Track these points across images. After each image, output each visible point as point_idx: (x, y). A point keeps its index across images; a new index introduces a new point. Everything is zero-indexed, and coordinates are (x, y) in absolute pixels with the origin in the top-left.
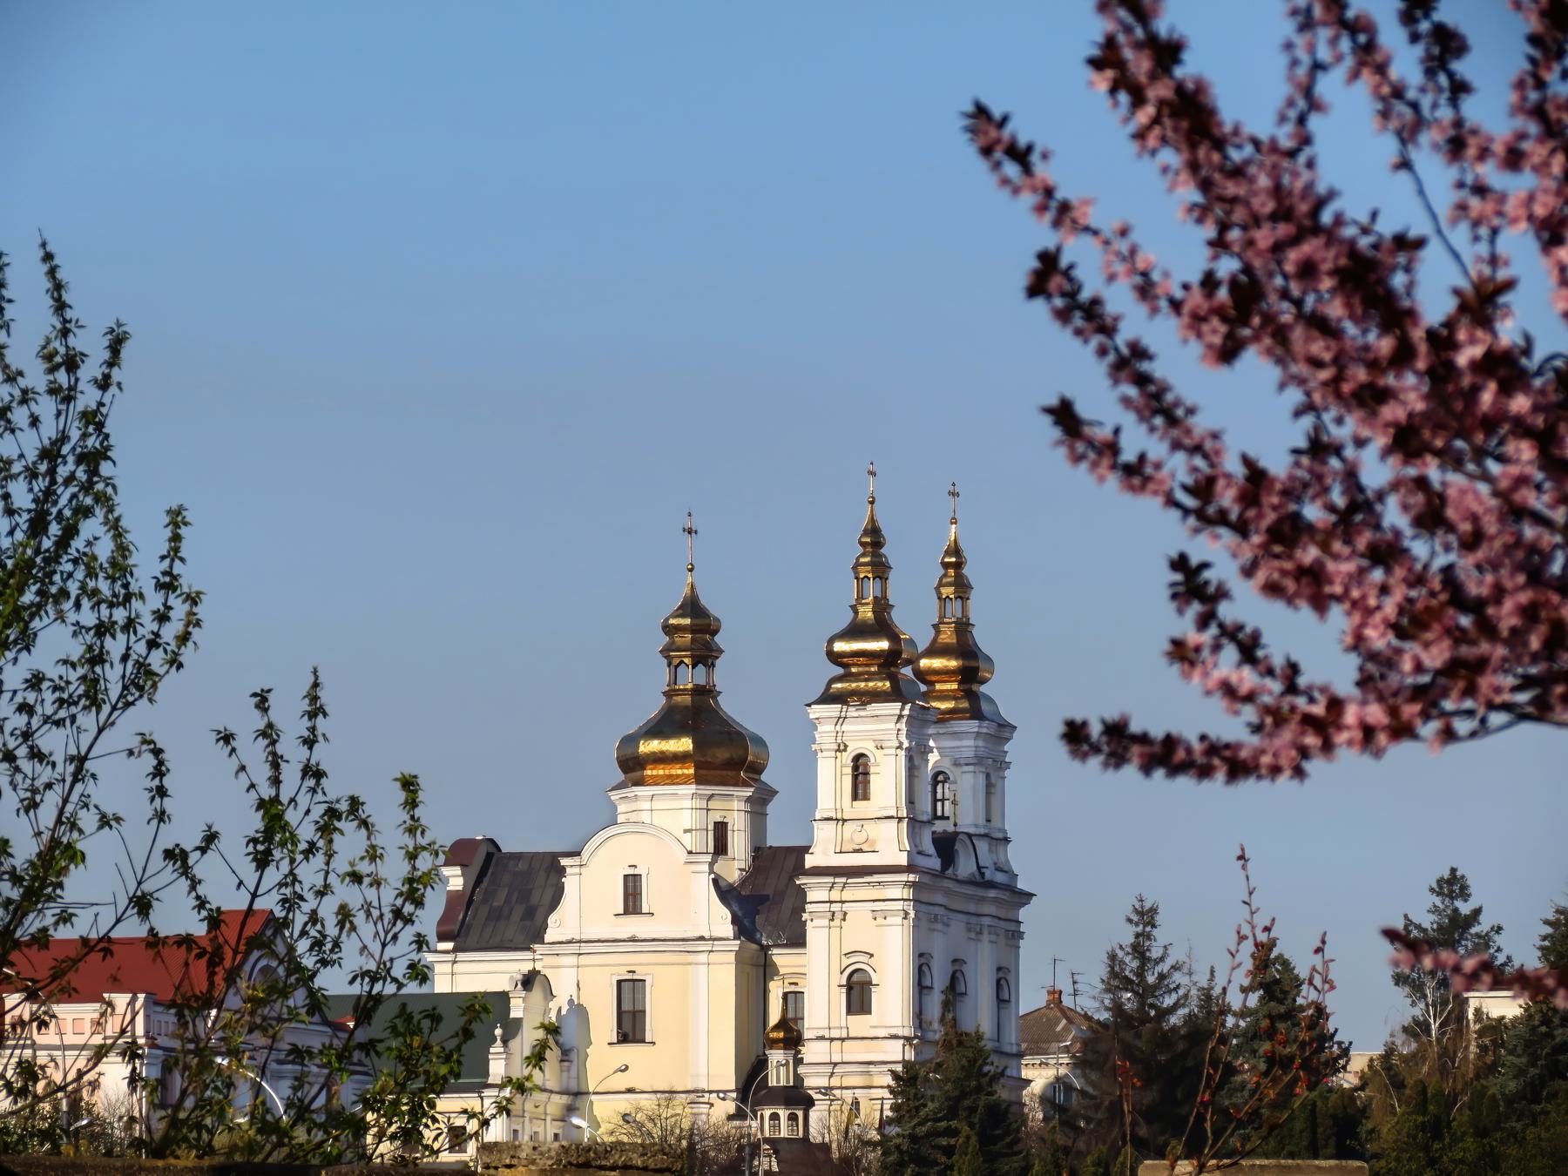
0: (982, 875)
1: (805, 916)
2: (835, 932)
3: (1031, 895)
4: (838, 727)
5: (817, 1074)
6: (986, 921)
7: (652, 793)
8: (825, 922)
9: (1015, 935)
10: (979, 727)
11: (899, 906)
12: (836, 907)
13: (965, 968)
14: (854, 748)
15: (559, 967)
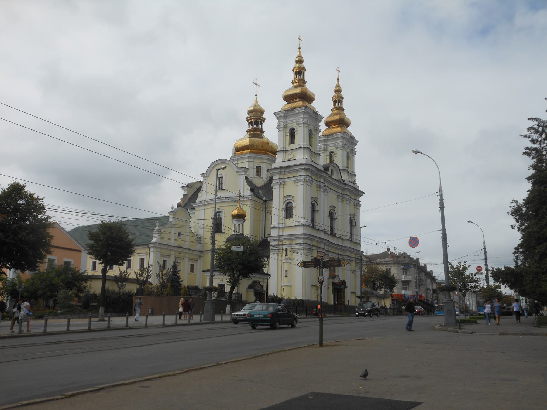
0: (344, 181)
1: (272, 185)
2: (282, 189)
3: (364, 193)
4: (285, 120)
5: (274, 240)
6: (345, 196)
7: (237, 158)
8: (278, 186)
9: (357, 205)
10: (343, 135)
11: (302, 177)
12: (282, 181)
13: (336, 210)
15: (199, 210)
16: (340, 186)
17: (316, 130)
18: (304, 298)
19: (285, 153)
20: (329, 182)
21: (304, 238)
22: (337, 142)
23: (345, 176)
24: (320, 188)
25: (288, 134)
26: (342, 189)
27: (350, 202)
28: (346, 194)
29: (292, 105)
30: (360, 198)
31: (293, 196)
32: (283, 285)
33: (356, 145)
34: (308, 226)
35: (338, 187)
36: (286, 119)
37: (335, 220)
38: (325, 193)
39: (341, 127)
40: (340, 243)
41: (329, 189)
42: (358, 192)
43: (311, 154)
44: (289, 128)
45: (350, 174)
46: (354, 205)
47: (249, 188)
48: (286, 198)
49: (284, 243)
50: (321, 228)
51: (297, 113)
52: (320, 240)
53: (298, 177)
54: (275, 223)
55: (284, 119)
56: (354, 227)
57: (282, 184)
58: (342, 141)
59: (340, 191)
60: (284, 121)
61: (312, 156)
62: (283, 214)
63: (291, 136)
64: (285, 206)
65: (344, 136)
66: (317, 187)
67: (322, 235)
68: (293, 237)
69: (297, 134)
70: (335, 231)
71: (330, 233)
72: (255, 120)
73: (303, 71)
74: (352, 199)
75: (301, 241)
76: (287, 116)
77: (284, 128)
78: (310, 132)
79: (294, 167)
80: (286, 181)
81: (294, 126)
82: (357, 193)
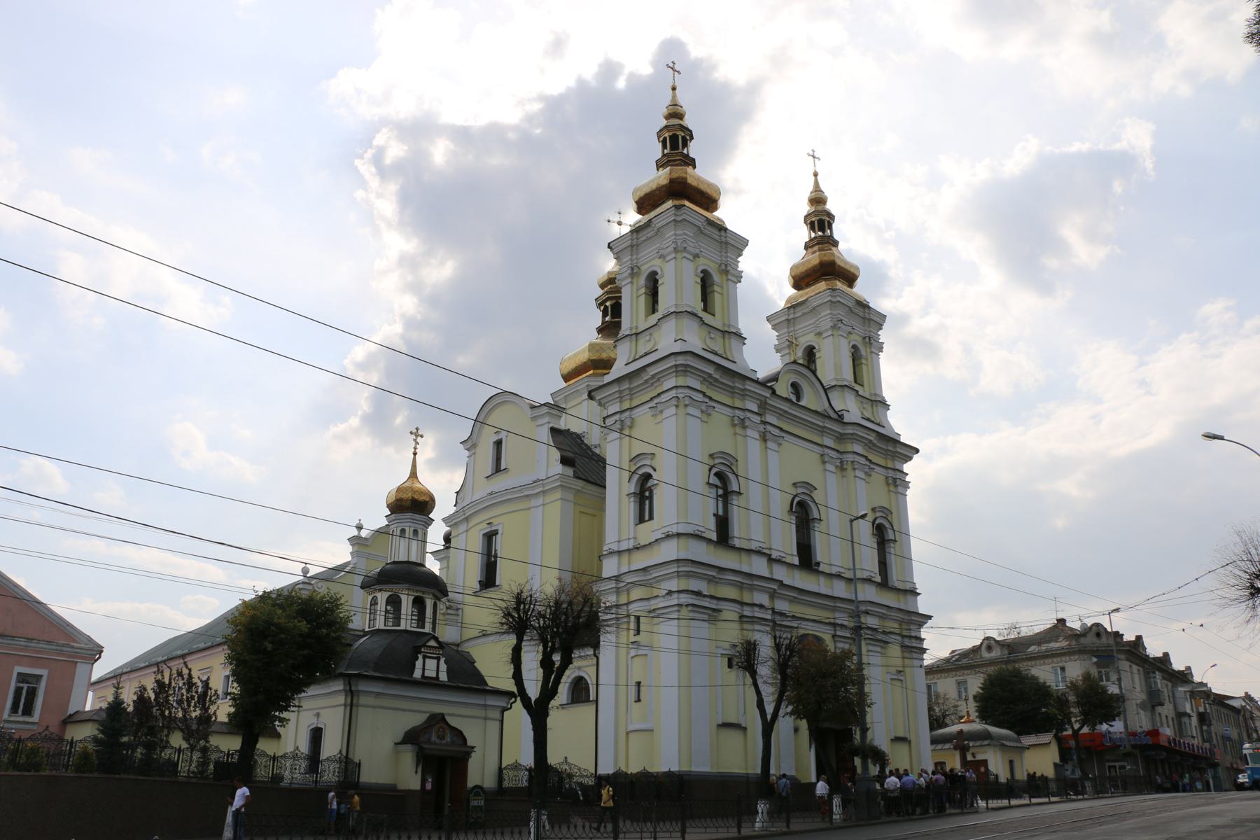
0: (841, 417)
3: (917, 451)
4: (635, 256)
6: (850, 457)
7: (563, 396)
9: (898, 483)
11: (673, 393)
12: (627, 414)
13: (816, 495)
14: (646, 270)
16: (825, 427)
17: (726, 272)
18: (685, 768)
19: (634, 343)
20: (783, 414)
21: (679, 575)
22: (818, 320)
23: (851, 408)
24: (744, 427)
25: (643, 290)
26: (837, 437)
27: (866, 473)
28: (851, 450)
29: (653, 214)
30: (905, 465)
31: (654, 454)
32: (631, 728)
33: (880, 326)
34: (697, 536)
35: (823, 431)
36: (637, 254)
37: (816, 525)
38: (770, 444)
39: (826, 280)
40: (840, 589)
41: (784, 435)
42: (895, 447)
43: (710, 333)
44: (646, 272)
45: (865, 401)
46: (888, 484)
47: (556, 455)
48: (635, 464)
49: (632, 599)
50: (754, 546)
52: (745, 581)
53: (663, 396)
54: (611, 539)
55: (632, 255)
56: (892, 545)
57: (624, 427)
58: (831, 314)
59: (828, 441)
61: (712, 338)
62: (630, 507)
63: (652, 294)
64: (636, 487)
65: (834, 300)
66: (734, 425)
67: (759, 566)
68: (651, 574)
70: (820, 554)
71: (796, 561)
72: (614, 301)
73: (683, 134)
74: (872, 466)
75: (673, 585)
76: (638, 245)
77: (632, 278)
78: (702, 275)
79: (649, 369)
80: (635, 416)
81: (655, 266)
82: (890, 448)
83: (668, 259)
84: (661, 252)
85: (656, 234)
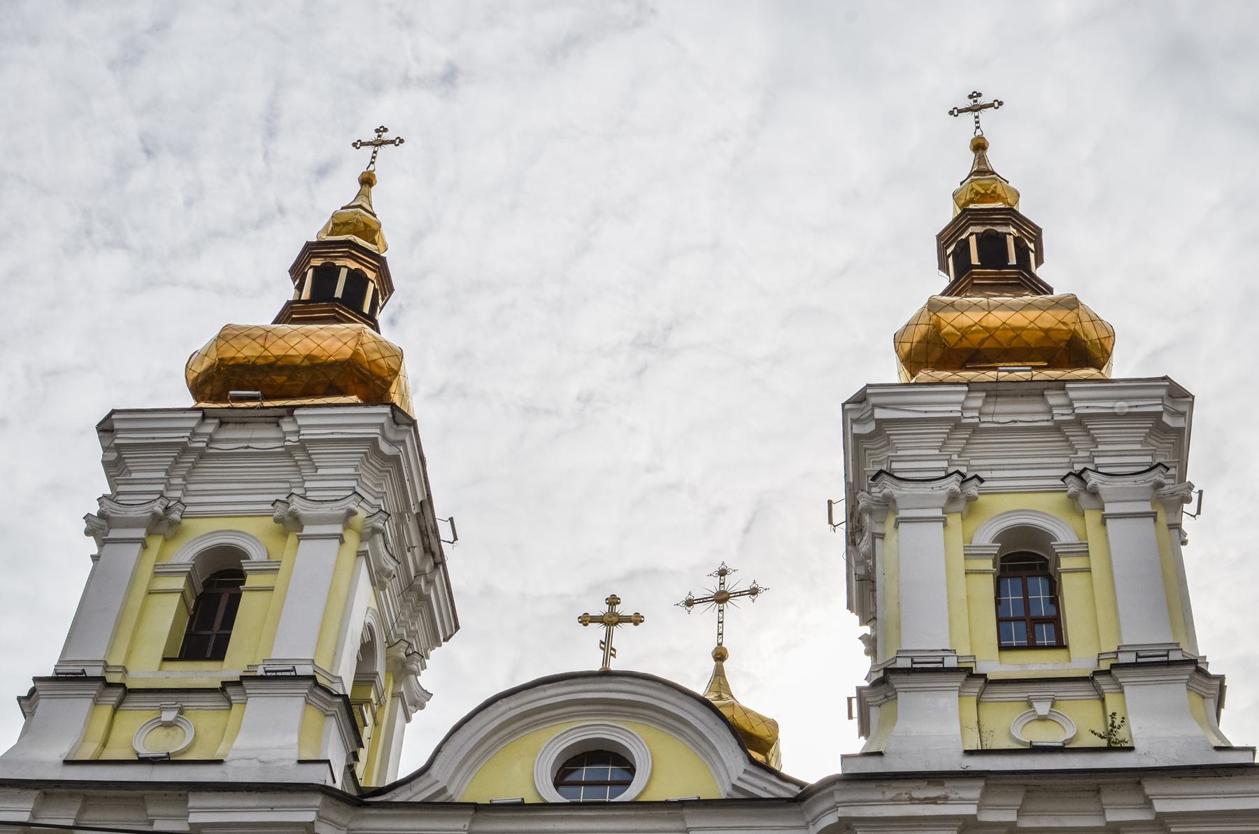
19: (106, 711)
25: (180, 583)
51: (303, 445)
60: (169, 487)
69: (271, 589)
76: (202, 455)
77: (149, 534)
79: (194, 801)
83: (307, 530)
84: (297, 505)
85: (288, 453)
